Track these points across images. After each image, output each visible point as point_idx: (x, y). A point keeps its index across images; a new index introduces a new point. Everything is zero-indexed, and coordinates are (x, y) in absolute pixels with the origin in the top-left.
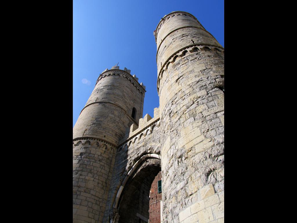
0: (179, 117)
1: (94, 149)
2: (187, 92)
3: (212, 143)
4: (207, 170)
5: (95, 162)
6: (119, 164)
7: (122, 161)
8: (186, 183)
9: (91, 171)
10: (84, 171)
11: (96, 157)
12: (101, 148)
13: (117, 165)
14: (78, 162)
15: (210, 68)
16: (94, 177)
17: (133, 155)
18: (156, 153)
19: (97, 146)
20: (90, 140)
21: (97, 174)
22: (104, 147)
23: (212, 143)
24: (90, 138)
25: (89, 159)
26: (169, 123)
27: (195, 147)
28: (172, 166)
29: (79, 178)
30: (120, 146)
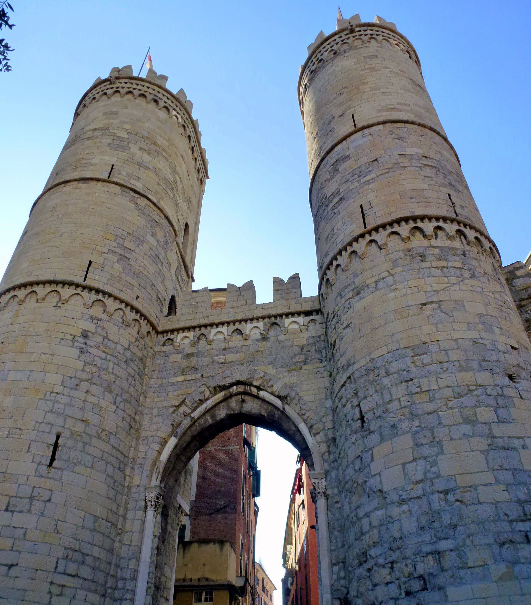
0: (436, 407)
1: (116, 329)
2: (454, 356)
3: (506, 496)
4: (502, 539)
5: (118, 365)
6: (165, 381)
7: (175, 376)
8: (461, 544)
9: (109, 385)
10: (94, 384)
11: (120, 352)
12: (129, 329)
13: (159, 381)
14: (79, 356)
15: (492, 316)
16: (117, 404)
17: (209, 374)
18: (272, 394)
19: (121, 321)
20: (102, 299)
21: (121, 396)
22: (135, 326)
23: (506, 496)
24: (104, 293)
25: (105, 352)
26: (404, 403)
27: (476, 489)
28: (419, 498)
29: (85, 401)
30: (167, 332)
